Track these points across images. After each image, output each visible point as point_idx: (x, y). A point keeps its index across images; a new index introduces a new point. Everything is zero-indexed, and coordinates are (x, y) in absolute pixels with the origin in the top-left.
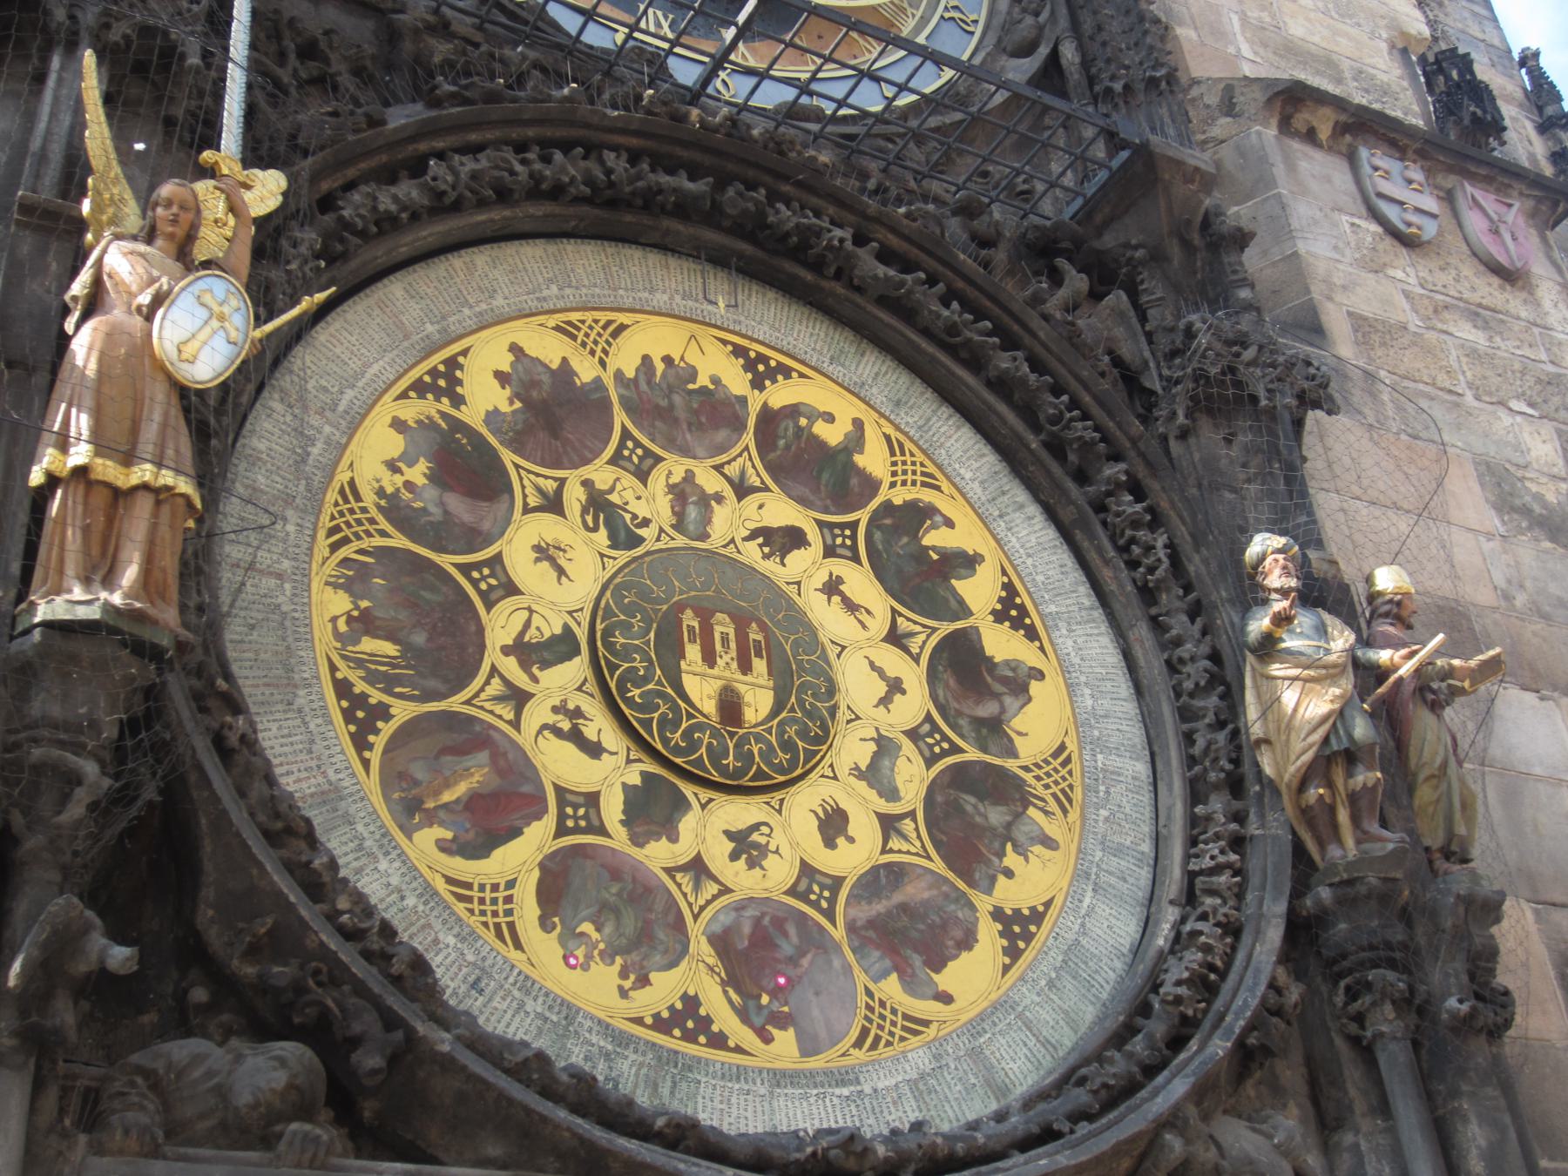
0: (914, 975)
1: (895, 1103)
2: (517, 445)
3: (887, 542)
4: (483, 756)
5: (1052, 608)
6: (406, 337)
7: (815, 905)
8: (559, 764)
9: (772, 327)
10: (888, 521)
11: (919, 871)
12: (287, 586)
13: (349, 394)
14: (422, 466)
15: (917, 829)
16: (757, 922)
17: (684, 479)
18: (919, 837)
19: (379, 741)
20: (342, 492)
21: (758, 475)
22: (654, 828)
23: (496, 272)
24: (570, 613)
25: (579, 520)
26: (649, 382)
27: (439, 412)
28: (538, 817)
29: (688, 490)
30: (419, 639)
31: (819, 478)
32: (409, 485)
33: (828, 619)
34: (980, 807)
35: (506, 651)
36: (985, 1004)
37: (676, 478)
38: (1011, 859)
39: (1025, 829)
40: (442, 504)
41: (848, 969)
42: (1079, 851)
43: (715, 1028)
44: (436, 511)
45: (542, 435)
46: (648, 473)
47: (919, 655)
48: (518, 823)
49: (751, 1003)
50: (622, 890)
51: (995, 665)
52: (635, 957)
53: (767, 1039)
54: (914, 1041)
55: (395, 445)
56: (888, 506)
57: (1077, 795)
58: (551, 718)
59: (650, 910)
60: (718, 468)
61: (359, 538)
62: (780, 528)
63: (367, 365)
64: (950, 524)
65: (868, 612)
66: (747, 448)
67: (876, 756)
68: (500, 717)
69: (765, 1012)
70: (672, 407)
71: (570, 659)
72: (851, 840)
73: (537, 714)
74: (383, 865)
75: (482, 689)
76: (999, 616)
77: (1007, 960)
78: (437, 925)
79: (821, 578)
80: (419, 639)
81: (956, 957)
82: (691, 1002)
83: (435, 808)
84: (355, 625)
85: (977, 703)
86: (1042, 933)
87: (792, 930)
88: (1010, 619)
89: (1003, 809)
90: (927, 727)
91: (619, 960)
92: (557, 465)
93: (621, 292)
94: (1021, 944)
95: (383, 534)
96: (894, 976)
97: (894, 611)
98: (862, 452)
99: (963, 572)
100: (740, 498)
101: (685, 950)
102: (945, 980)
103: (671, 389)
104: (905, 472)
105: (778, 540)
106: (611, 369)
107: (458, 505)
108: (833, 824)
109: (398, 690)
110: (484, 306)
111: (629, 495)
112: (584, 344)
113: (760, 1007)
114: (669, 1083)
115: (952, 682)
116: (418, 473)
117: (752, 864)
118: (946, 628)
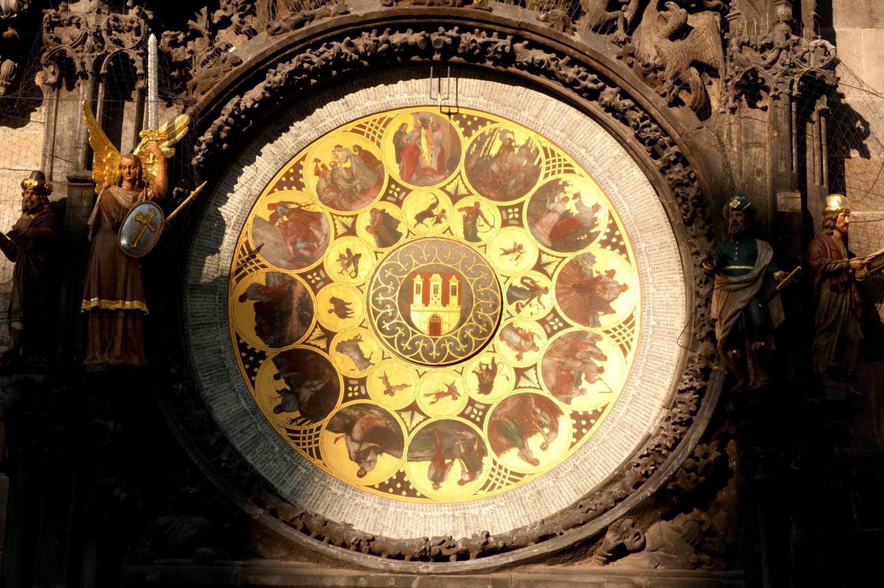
2: (574, 264)
3: (464, 439)
4: (435, 166)
5: (391, 509)
6: (640, 230)
8: (419, 198)
9: (605, 441)
10: (476, 447)
11: (301, 334)
12: (532, 118)
13: (616, 189)
14: (575, 211)
15: (319, 347)
16: (317, 241)
17: (534, 345)
18: (315, 346)
19: (456, 124)
20: (569, 165)
21: (525, 387)
22: (376, 223)
24: (485, 245)
25: (529, 276)
26: (591, 353)
28: (401, 174)
30: (494, 167)
31: (512, 420)
32: (566, 199)
33: (439, 378)
34: (312, 389)
35: (477, 204)
36: (230, 314)
37: (536, 338)
38: (282, 384)
40: (554, 211)
41: (278, 265)
42: (266, 420)
43: (285, 188)
44: (551, 206)
45: (577, 280)
46: (543, 326)
47: (400, 415)
48: (402, 164)
49: (287, 211)
51: (377, 453)
52: (328, 176)
53: (271, 206)
55: (588, 202)
56: (483, 452)
58: (440, 207)
59: (344, 196)
60: (535, 366)
61: (548, 163)
62: (492, 382)
63: (629, 203)
64: (462, 482)
65: (433, 403)
66: (541, 389)
67: (361, 355)
68: (449, 184)
70: (575, 359)
71: (465, 233)
72: (330, 311)
73: (445, 202)
74: (406, 96)
75: (463, 183)
76: (401, 475)
77: (241, 341)
78: (375, 102)
79: (460, 390)
80: (494, 167)
81: (256, 319)
82: (300, 186)
83: (420, 133)
84: (508, 141)
85: (362, 428)
86: (243, 368)
87: (307, 253)
88: (397, 481)
89: (306, 400)
90: (363, 392)
91: (330, 169)
92: (560, 280)
93: (645, 361)
94: (244, 354)
95: (546, 176)
96: (264, 284)
97: (428, 418)
98: (519, 455)
99: (433, 472)
102: (250, 304)
103: (583, 363)
104: (499, 474)
105: (488, 377)
106: (603, 335)
107: (552, 219)
108: (341, 309)
109: (475, 145)
110: (651, 280)
111: (534, 309)
112: (620, 327)
113: (284, 214)
115: (379, 422)
116: (571, 206)
117: (341, 256)
118: (408, 440)
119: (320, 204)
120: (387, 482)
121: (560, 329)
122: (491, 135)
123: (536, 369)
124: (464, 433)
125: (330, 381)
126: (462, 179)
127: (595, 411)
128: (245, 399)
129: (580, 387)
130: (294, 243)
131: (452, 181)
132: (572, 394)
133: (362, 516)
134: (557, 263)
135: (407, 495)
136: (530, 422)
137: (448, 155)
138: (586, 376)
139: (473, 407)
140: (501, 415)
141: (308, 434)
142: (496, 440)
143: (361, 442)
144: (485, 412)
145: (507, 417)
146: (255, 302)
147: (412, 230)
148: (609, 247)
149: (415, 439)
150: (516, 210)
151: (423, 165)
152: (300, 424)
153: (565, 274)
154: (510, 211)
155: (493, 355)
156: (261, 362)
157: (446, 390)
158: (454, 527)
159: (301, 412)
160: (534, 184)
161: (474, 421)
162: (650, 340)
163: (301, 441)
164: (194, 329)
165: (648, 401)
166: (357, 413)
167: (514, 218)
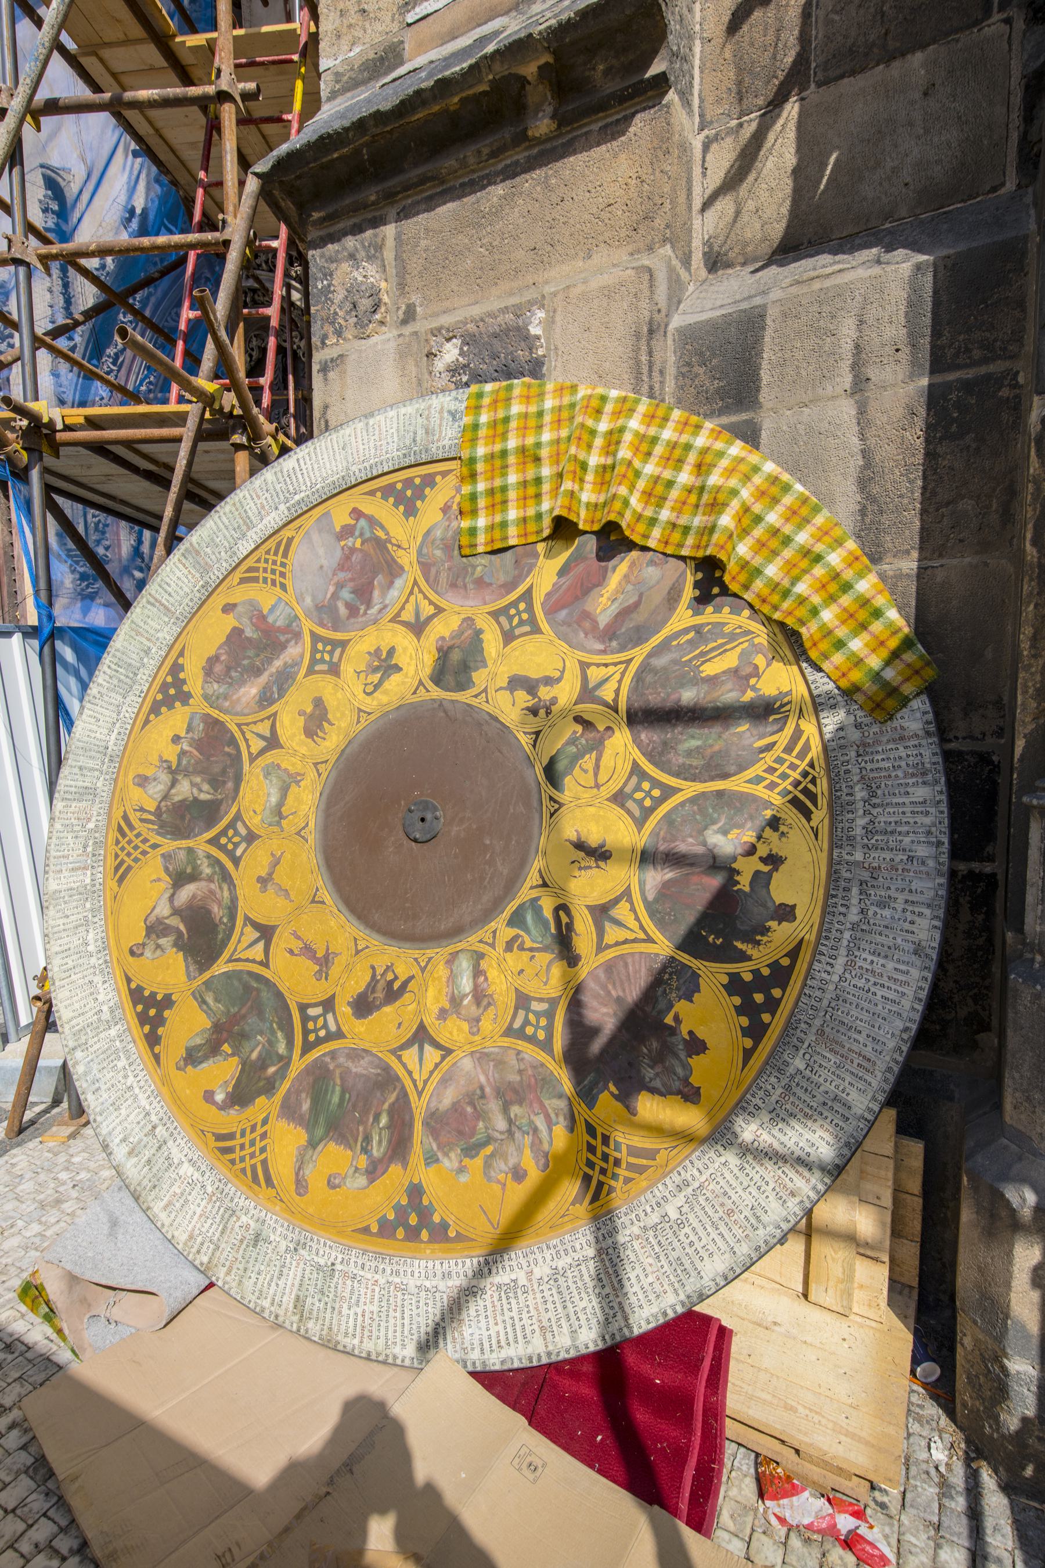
0: (251, 619)
1: (263, 507)
3: (271, 1043)
4: (603, 620)
5: (113, 1032)
6: (821, 1032)
7: (327, 641)
9: (404, 1289)
10: (272, 1070)
13: (853, 916)
15: (248, 747)
16: (369, 606)
17: (478, 1020)
18: (246, 740)
20: (813, 797)
23: (749, 1201)
26: (536, 1130)
27: (749, 958)
28: (548, 595)
29: (474, 1011)
34: (195, 791)
39: (161, 787)
41: (300, 599)
43: (391, 500)
47: (245, 925)
48: (563, 580)
49: (368, 535)
50: (473, 574)
51: (175, 945)
54: (250, 562)
55: (781, 891)
57: (113, 834)
61: (780, 761)
62: (378, 1008)
63: (849, 965)
65: (291, 952)
68: (598, 665)
69: (357, 533)
70: (505, 1109)
72: (302, 713)
75: (620, 682)
76: (168, 1002)
79: (335, 971)
82: (411, 511)
84: (749, 670)
85: (194, 896)
87: (343, 611)
89: (177, 799)
92: (609, 967)
94: (169, 679)
95: (757, 780)
96: (265, 612)
99: (199, 1041)
100: (422, 1027)
101: (419, 553)
102: (230, 622)
103: (510, 1133)
105: (380, 995)
108: (316, 721)
114: (418, 439)
115: (215, 909)
117: (378, 650)
118: (221, 967)
119: (414, 557)
120: (147, 993)
121: (532, 1040)
122: (732, 637)
123: (443, 1058)
124: (279, 1034)
125: (221, 801)
126: (623, 674)
127: (444, 1226)
128: (119, 733)
129: (466, 1161)
130: (340, 586)
131: (606, 665)
132: (446, 1155)
133: (82, 1004)
134: (631, 936)
135: (146, 1036)
136: (361, 1122)
137: (639, 617)
138: (492, 1155)
139: (324, 1015)
140: (338, 1066)
141: (137, 841)
142: (298, 1093)
143: (176, 912)
144: (330, 1037)
145: (342, 1078)
146: (237, 624)
147: (491, 692)
148: (737, 1000)
149: (227, 975)
150: (656, 793)
151: (588, 607)
152: (142, 820)
153: (626, 965)
154: (646, 786)
155: (415, 970)
156: (178, 704)
157: (320, 954)
158: (139, 1142)
159: (158, 808)
160: (725, 776)
161: (306, 1032)
162: (636, 1230)
163: (123, 842)
164: (149, 602)
165: (526, 1322)
166: (207, 871)
167: (640, 803)
